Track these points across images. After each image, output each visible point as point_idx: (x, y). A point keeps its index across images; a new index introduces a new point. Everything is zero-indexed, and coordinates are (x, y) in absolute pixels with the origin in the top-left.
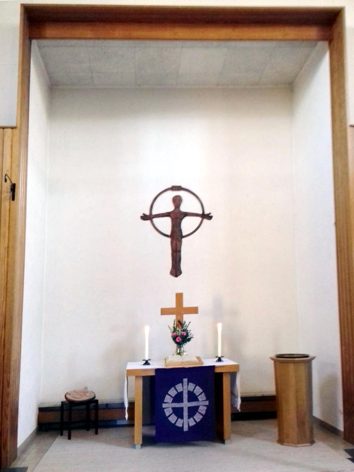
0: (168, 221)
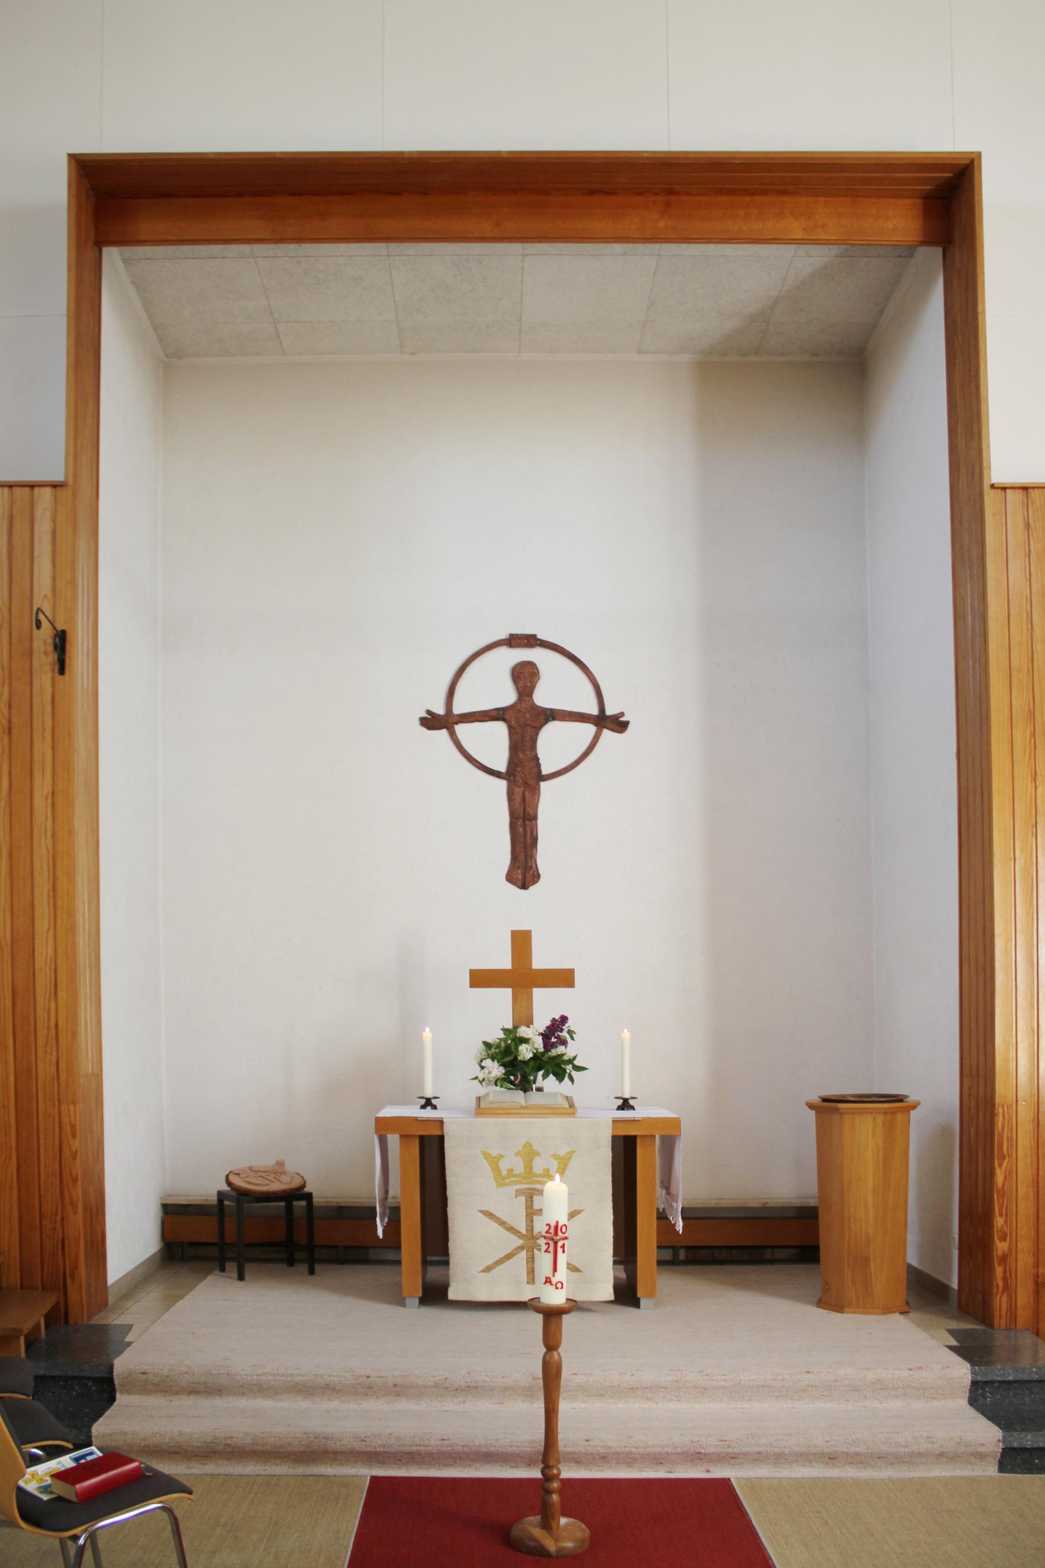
0: (499, 731)
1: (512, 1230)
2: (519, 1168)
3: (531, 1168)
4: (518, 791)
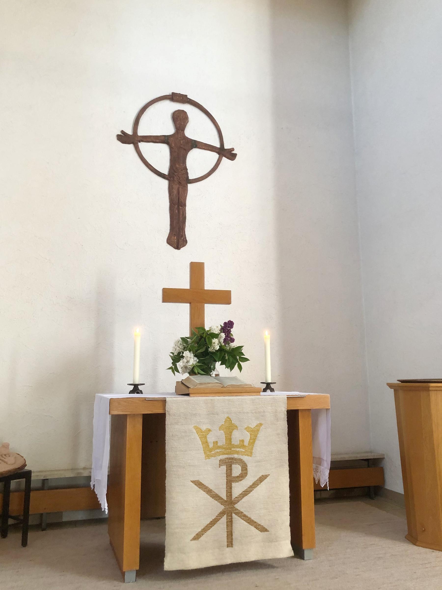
1: (216, 497)
2: (222, 442)
3: (230, 439)
4: (176, 187)
